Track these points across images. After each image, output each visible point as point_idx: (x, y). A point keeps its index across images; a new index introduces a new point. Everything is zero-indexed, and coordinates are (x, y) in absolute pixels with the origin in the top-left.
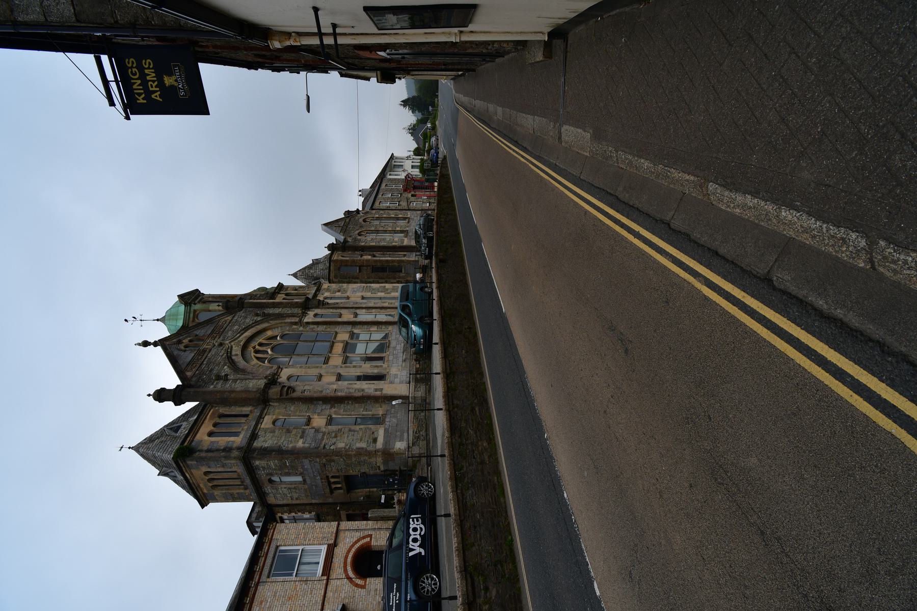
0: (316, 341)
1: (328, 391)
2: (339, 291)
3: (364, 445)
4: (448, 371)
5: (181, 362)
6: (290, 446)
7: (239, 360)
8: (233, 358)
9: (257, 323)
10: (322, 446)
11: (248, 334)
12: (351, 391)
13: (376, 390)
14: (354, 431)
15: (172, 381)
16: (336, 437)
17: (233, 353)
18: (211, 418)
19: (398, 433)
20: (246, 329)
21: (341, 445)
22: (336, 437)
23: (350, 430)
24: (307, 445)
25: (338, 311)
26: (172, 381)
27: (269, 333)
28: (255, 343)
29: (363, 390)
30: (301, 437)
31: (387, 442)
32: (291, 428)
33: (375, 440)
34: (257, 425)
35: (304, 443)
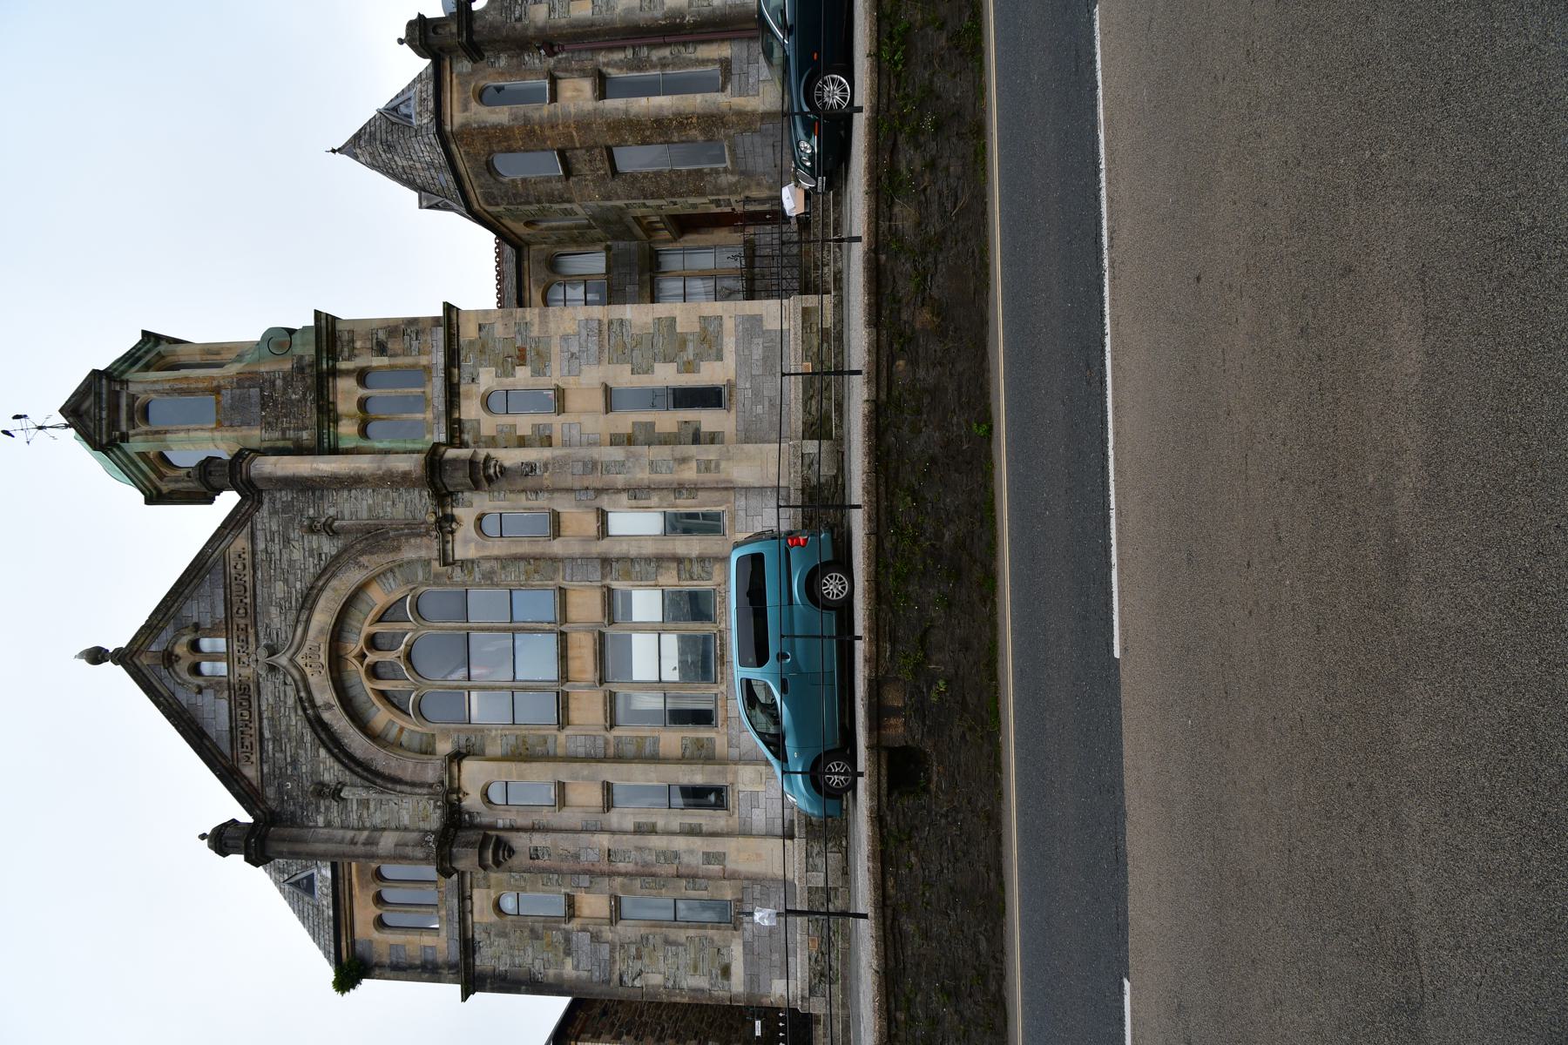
0: (514, 631)
1: (593, 856)
2: (522, 359)
3: (701, 982)
5: (212, 733)
6: (551, 972)
7: (337, 720)
8: (326, 716)
9: (330, 569)
10: (616, 977)
11: (322, 618)
12: (651, 858)
13: (709, 857)
14: (675, 943)
15: (232, 810)
16: (639, 957)
17: (319, 701)
18: (363, 886)
19: (776, 957)
20: (308, 601)
21: (656, 979)
22: (639, 957)
23: (667, 942)
24: (584, 974)
25: (543, 501)
26: (232, 810)
27: (379, 597)
28: (355, 644)
29: (676, 855)
30: (568, 953)
31: (752, 979)
32: (539, 926)
33: (726, 972)
34: (462, 920)
35: (576, 968)
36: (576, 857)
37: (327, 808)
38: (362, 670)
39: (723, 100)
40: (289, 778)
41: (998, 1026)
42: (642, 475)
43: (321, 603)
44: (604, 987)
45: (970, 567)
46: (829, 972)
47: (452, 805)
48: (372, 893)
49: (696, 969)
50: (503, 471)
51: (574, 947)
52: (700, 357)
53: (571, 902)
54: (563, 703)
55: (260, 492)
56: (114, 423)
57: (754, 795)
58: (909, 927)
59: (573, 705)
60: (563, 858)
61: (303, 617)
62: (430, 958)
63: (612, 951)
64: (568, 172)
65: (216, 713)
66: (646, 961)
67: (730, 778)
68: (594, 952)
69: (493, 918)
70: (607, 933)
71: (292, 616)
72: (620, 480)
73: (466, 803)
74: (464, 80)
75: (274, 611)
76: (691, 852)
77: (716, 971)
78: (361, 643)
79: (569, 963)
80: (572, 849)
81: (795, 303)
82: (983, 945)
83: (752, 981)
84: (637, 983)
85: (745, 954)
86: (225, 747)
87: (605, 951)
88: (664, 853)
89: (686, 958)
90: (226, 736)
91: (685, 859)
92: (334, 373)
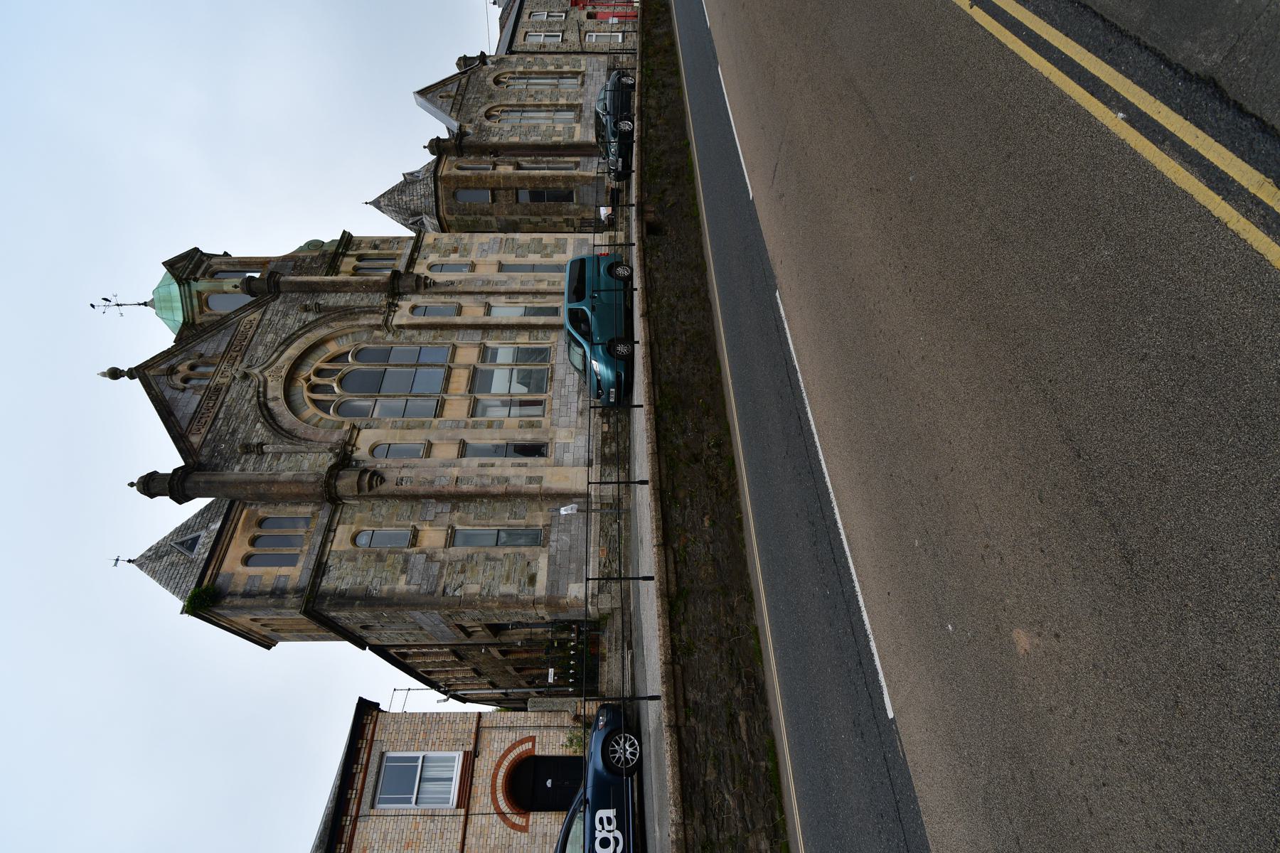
0: (417, 365)
1: (444, 482)
2: (455, 250)
3: (511, 589)
4: (673, 589)
5: (179, 415)
6: (386, 588)
7: (279, 407)
8: (271, 404)
9: (307, 327)
10: (440, 589)
11: (293, 351)
12: (487, 481)
13: (531, 480)
14: (495, 559)
15: (169, 460)
16: (463, 571)
17: (270, 394)
18: (245, 529)
19: (573, 566)
20: (288, 342)
21: (473, 589)
22: (463, 571)
23: (488, 558)
24: (413, 588)
25: (455, 299)
26: (169, 460)
27: (333, 348)
28: (307, 371)
29: (507, 480)
30: (404, 571)
31: (553, 584)
32: (385, 551)
33: (532, 580)
34: (323, 545)
35: (408, 583)
36: (432, 482)
37: (246, 461)
38: (305, 386)
39: (575, 172)
40: (225, 442)
41: (778, 833)
42: (516, 287)
43: (295, 344)
44: (429, 598)
45: (683, 174)
46: (618, 574)
47: (345, 454)
48: (250, 535)
49: (508, 578)
50: (435, 283)
51: (410, 566)
52: (553, 252)
53: (415, 534)
54: (441, 405)
55: (280, 292)
56: (194, 272)
57: (566, 446)
58: (657, 275)
59: (447, 407)
60: (422, 484)
61: (281, 348)
62: (281, 585)
63: (442, 567)
64: (494, 200)
65: (189, 402)
66: (468, 574)
67: (550, 435)
68: (426, 570)
69: (349, 546)
70: (441, 556)
71: (270, 352)
72: (503, 289)
73: (356, 455)
74: (451, 162)
75: (260, 348)
76: (518, 477)
77: (525, 579)
78: (311, 371)
79: (403, 578)
80: (429, 478)
81: (606, 235)
82: (697, 281)
83: (552, 585)
84: (457, 593)
85: (549, 565)
86: (184, 424)
87: (435, 568)
88: (498, 478)
89: (502, 570)
90: (189, 416)
91: (513, 481)
92: (344, 255)
